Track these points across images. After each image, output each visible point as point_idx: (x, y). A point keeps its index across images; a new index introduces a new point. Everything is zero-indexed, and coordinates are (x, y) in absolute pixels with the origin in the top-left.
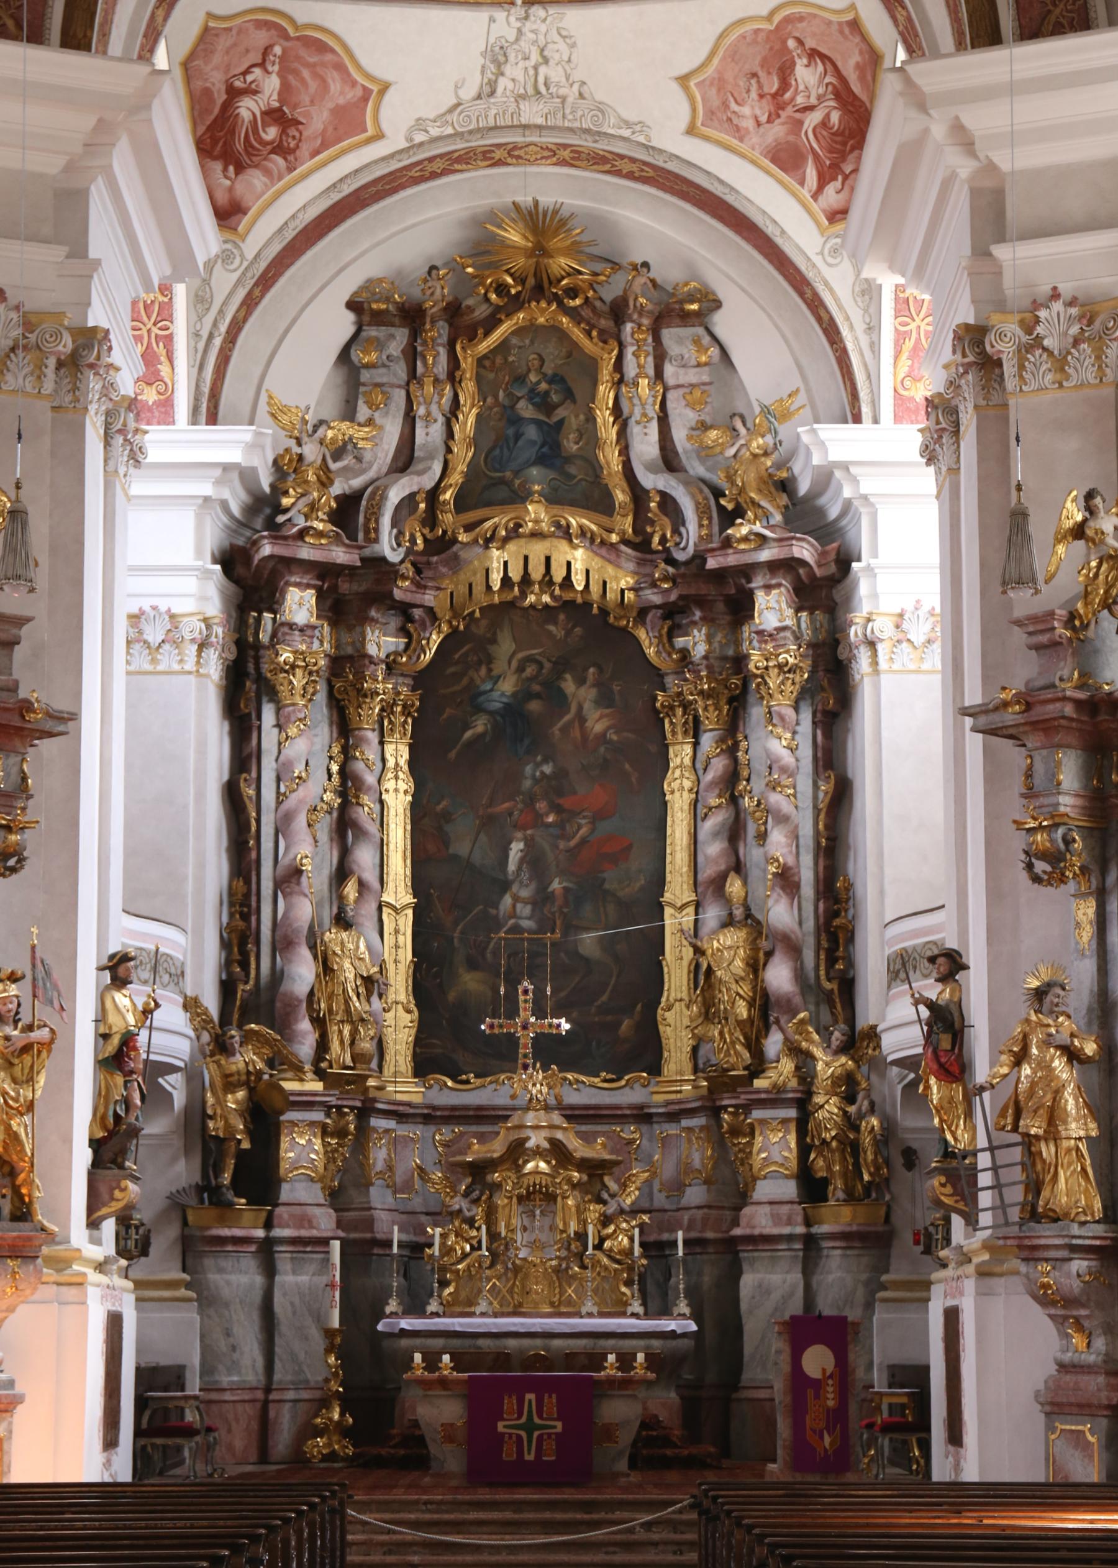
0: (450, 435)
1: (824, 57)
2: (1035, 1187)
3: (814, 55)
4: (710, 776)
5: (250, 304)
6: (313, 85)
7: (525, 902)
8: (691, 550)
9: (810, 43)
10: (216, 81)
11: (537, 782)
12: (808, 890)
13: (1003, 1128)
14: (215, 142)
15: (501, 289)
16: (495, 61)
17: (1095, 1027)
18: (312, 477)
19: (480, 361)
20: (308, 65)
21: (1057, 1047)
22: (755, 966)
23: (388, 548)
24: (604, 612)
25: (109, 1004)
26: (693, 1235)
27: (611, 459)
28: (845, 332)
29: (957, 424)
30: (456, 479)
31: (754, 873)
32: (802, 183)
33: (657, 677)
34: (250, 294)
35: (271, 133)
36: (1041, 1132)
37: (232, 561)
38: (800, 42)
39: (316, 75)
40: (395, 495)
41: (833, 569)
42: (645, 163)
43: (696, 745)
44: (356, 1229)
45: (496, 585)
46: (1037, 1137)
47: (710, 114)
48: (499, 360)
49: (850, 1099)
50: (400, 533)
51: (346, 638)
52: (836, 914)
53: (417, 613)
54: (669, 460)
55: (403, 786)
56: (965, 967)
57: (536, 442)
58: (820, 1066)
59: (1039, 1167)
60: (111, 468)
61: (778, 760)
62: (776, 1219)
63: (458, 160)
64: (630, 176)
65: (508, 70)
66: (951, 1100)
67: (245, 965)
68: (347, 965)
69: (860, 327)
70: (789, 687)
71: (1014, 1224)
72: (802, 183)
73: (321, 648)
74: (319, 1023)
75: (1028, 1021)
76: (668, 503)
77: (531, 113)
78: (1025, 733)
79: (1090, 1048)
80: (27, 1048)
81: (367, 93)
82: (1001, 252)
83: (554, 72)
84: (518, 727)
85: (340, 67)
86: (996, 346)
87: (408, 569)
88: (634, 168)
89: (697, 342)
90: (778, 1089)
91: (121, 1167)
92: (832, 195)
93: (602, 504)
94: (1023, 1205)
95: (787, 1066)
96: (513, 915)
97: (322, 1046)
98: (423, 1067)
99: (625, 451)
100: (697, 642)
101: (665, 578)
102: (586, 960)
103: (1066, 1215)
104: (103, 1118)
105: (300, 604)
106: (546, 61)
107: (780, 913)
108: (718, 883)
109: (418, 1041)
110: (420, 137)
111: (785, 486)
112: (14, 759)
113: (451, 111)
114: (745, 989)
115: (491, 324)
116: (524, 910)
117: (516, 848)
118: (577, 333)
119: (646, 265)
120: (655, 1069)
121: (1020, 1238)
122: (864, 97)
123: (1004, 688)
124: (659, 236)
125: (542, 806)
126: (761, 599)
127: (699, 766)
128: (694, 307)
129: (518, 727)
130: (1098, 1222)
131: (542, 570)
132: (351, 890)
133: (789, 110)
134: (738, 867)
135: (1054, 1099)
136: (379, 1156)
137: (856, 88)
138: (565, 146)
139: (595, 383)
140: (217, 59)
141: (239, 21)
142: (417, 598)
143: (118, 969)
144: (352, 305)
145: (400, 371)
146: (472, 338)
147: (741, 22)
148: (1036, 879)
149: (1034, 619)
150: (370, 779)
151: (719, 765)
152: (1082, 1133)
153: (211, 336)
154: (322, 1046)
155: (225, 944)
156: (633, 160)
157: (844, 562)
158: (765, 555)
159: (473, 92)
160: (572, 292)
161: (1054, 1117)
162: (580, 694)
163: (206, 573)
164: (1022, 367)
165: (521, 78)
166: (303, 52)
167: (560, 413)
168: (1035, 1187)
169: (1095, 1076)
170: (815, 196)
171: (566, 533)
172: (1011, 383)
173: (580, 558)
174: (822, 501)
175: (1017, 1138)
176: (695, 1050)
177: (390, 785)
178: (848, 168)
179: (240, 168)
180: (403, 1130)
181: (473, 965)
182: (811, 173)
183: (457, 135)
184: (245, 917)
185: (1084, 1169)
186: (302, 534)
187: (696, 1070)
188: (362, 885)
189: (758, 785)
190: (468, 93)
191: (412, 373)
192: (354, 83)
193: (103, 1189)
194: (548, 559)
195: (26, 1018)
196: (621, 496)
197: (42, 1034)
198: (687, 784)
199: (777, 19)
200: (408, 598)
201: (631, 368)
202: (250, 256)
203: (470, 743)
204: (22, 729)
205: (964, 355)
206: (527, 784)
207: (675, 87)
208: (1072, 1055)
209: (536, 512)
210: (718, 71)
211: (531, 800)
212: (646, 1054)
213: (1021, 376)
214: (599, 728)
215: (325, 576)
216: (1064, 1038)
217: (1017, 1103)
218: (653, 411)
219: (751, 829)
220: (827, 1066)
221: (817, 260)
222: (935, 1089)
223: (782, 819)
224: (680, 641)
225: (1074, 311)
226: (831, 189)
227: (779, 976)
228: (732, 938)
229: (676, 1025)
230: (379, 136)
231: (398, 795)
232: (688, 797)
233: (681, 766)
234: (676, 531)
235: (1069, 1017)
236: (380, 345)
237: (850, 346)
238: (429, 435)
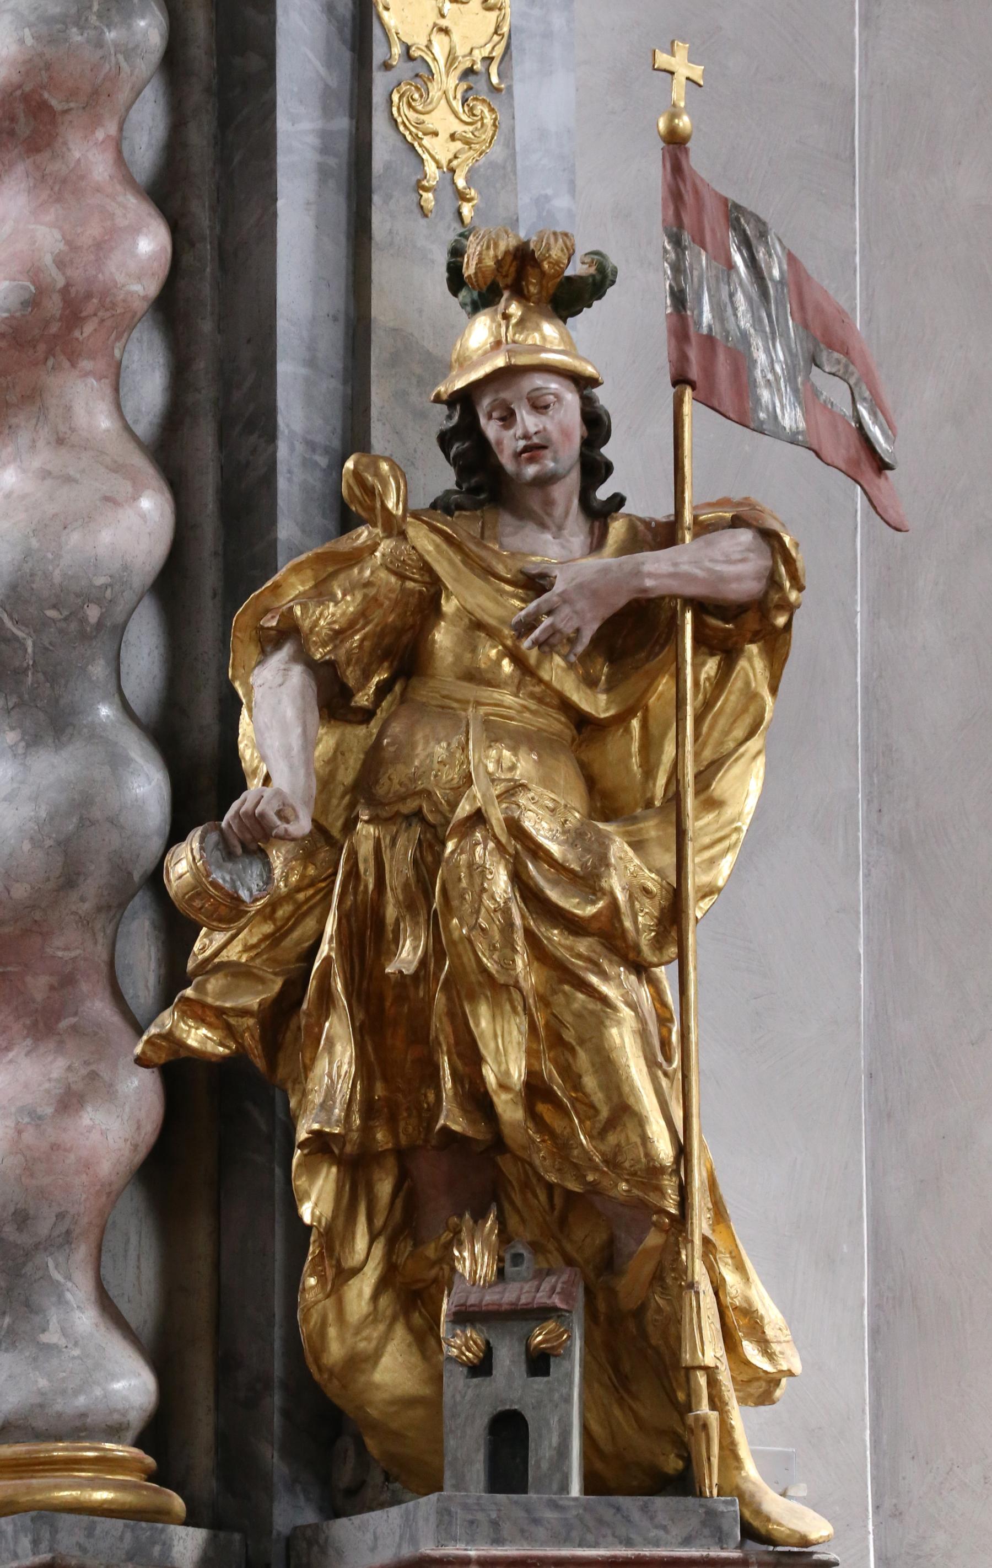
80: (634, 634)
197: (730, 563)
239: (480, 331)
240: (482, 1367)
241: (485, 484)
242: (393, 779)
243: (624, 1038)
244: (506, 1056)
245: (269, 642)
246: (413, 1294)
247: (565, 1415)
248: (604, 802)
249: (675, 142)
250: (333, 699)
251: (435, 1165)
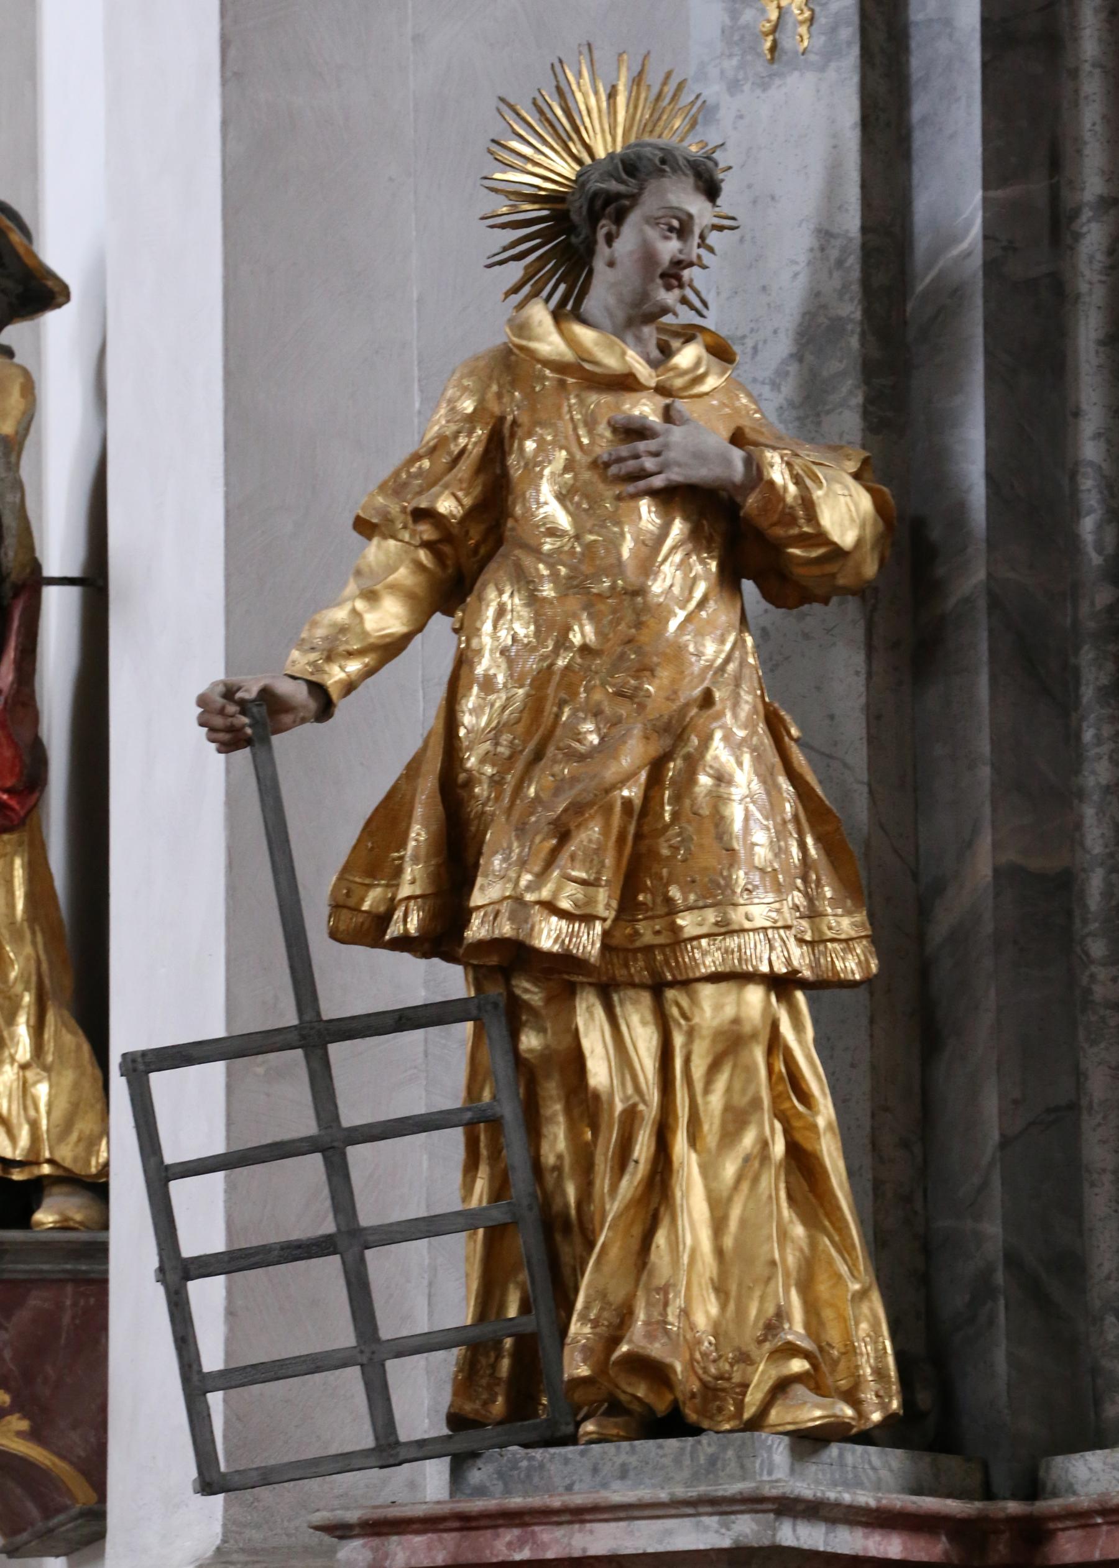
13: (372, 931)
17: (849, 421)
21: (669, 498)
36: (588, 942)
46: (563, 973)
59: (557, 1142)
71: (424, 1450)
75: (511, 364)
79: (845, 512)
94: (476, 1347)
103: (713, 1393)
121: (466, 1522)
130: (865, 1438)
135: (657, 767)
152: (800, 957)
161: (654, 855)
168: (535, 1241)
169: (845, 673)
175: (451, 981)
185: (802, 1162)
208: (742, 534)
216: (700, 445)
217: (453, 787)
235: (721, 352)
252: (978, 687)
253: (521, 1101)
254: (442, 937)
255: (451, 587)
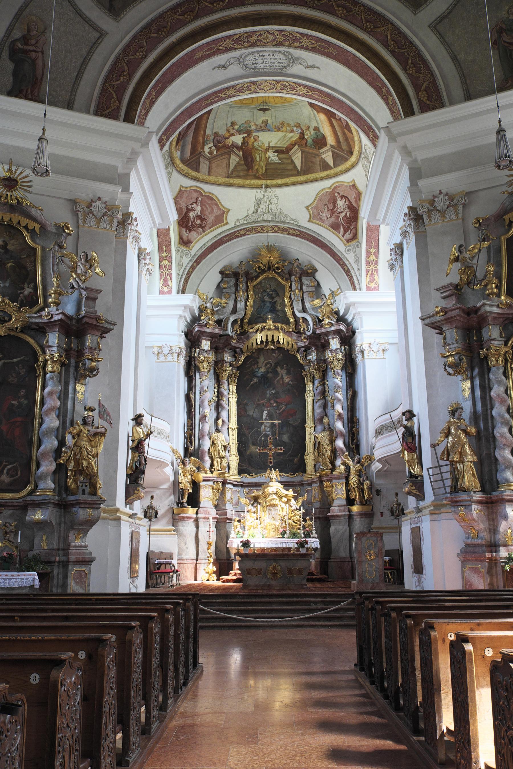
0: (246, 305)
1: (345, 197)
2: (455, 479)
3: (343, 197)
4: (318, 391)
5: (193, 268)
6: (210, 209)
7: (268, 427)
8: (311, 331)
9: (341, 194)
10: (184, 206)
11: (270, 395)
12: (346, 421)
13: (443, 459)
14: (183, 223)
15: (259, 268)
16: (257, 204)
17: (473, 424)
18: (209, 312)
19: (254, 287)
20: (208, 204)
21: (461, 430)
22: (332, 442)
23: (229, 331)
24: (288, 350)
25: (134, 430)
26: (317, 516)
27: (288, 311)
28: (352, 271)
29: (402, 252)
30: (248, 316)
31: (331, 417)
32: (339, 233)
33: (302, 367)
34: (193, 265)
35: (198, 222)
37: (188, 334)
38: (339, 193)
39: (210, 207)
40: (232, 319)
41: (351, 333)
42: (298, 230)
43: (313, 384)
44: (222, 515)
45: (259, 343)
47: (315, 216)
48: (259, 286)
49: (360, 476)
50: (233, 328)
51: (219, 356)
52: (354, 427)
53: (238, 350)
54: (304, 310)
55: (234, 396)
56: (414, 416)
57: (270, 306)
58: (351, 467)
59: (456, 473)
60: (140, 270)
61: (337, 384)
62: (340, 511)
63: (248, 231)
64: (293, 235)
65: (261, 206)
66: (413, 459)
67: (191, 443)
68: (219, 442)
69: (356, 270)
70: (339, 365)
72: (339, 233)
73: (212, 357)
74: (211, 458)
76: (305, 320)
77: (267, 217)
78: (443, 324)
79: (473, 430)
80: (95, 434)
81: (224, 212)
82: (421, 183)
83: (273, 207)
84: (266, 381)
85: (217, 205)
86: (420, 211)
87: (235, 337)
88: (294, 232)
89: (311, 280)
90: (340, 473)
91: (138, 483)
92: (348, 235)
93: (287, 322)
94: (452, 487)
95: (342, 467)
96: (265, 430)
97: (212, 465)
98: (241, 471)
99: (293, 309)
100: (313, 356)
101: (305, 339)
102: (285, 442)
103: (468, 489)
104: (132, 467)
105: (206, 344)
106: (271, 203)
107: (339, 425)
108: (321, 420)
109: (239, 465)
110: (238, 224)
111: (337, 313)
112: (95, 338)
113: (246, 217)
114: (329, 448)
115: (257, 277)
116: (268, 429)
117: (265, 413)
118: (279, 279)
119: (298, 259)
120: (304, 471)
122: (357, 207)
123: (437, 307)
124: (302, 251)
125: (272, 401)
126: (331, 341)
127: (315, 390)
128: (310, 271)
129: (266, 381)
131: (271, 338)
132: (220, 422)
133: (336, 214)
134: (326, 415)
136: (228, 495)
137: (354, 204)
138: (276, 226)
139: (284, 291)
140: (184, 199)
141: (189, 189)
142: (238, 345)
143: (138, 420)
144: (221, 272)
145: (233, 289)
146: (252, 280)
147: (323, 190)
148: (449, 374)
149: (444, 287)
150: (226, 393)
151: (320, 388)
153: (182, 275)
154: (212, 465)
155: (185, 437)
156: (294, 229)
157: (354, 333)
158: (332, 329)
159: (252, 212)
160: (278, 268)
161: (462, 454)
162: (282, 372)
163: (181, 335)
164: (430, 217)
165: (264, 208)
166: (206, 200)
167: (275, 299)
168: (455, 479)
169: (474, 441)
170: (343, 236)
171: (277, 329)
172: (426, 222)
173: (281, 336)
174: (346, 317)
175: (448, 463)
176: (315, 465)
177: (231, 396)
178: (352, 227)
179: (190, 231)
180: (235, 488)
181: (254, 444)
182: (342, 230)
183: (248, 223)
184: (191, 430)
185: (473, 474)
186: (206, 325)
187: (315, 471)
188: (223, 421)
189: (331, 393)
190: (250, 212)
191: (236, 290)
192: (220, 209)
193: (131, 491)
194: (273, 336)
195: (96, 424)
196: (292, 320)
197: (102, 430)
198: (311, 395)
199: (332, 187)
200: (236, 345)
201: (293, 288)
202: (193, 254)
203: (253, 385)
204: (98, 326)
205: (410, 216)
206: (268, 396)
207: (305, 209)
209: (270, 323)
210: (317, 204)
211: (269, 400)
212: (302, 467)
213: (430, 220)
214: (287, 380)
215: (212, 337)
217: (448, 450)
218: (300, 299)
219: (329, 405)
220: (354, 468)
221: (344, 253)
222: (407, 455)
223: (339, 400)
224: (308, 358)
225: (447, 197)
226: (347, 234)
227: (340, 443)
228: (326, 434)
229: (310, 459)
230: (227, 224)
231: (233, 399)
232: (312, 398)
233: (310, 390)
234: (307, 327)
236: (228, 282)
237: (353, 274)
238: (241, 305)
239: (86, 413)
240: (82, 486)
241: (85, 422)
242: (78, 444)
243: (93, 463)
244: (85, 464)
245: (69, 433)
246: (75, 481)
247: (87, 490)
248: (92, 446)
249: (99, 400)
250: (74, 438)
251: (79, 471)
252: (483, 441)
253: (454, 471)
254: (448, 460)
255: (447, 437)
